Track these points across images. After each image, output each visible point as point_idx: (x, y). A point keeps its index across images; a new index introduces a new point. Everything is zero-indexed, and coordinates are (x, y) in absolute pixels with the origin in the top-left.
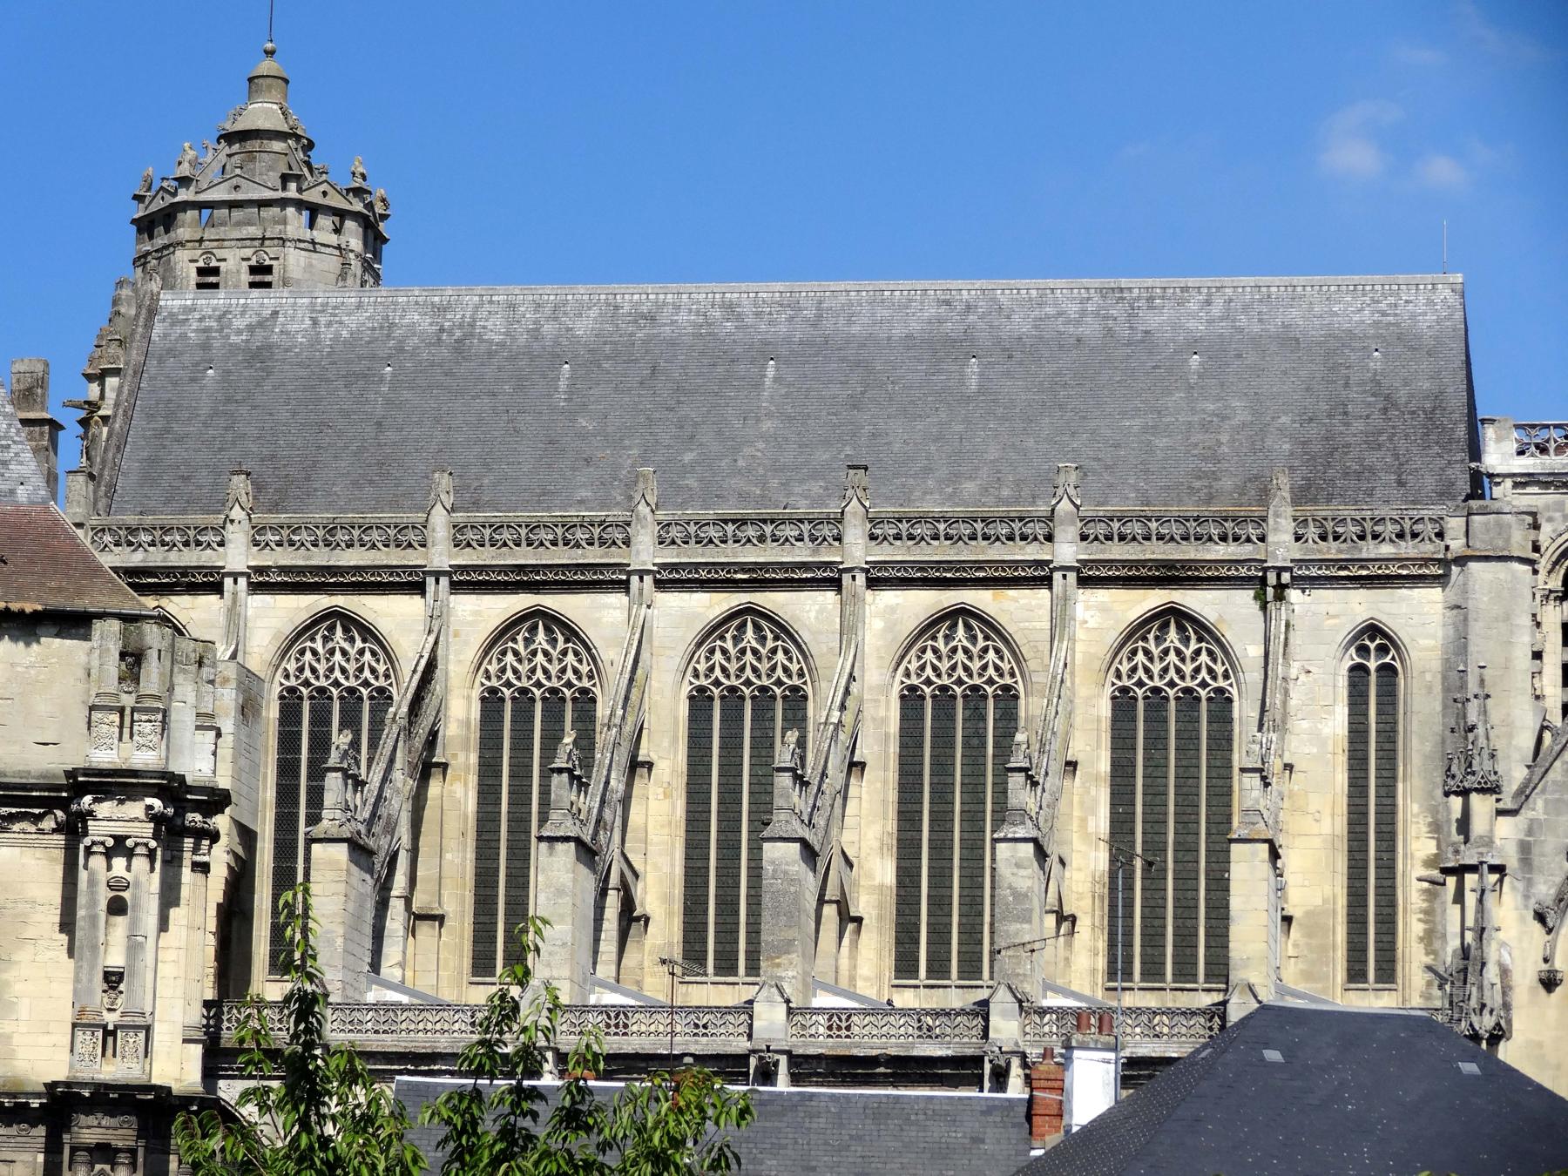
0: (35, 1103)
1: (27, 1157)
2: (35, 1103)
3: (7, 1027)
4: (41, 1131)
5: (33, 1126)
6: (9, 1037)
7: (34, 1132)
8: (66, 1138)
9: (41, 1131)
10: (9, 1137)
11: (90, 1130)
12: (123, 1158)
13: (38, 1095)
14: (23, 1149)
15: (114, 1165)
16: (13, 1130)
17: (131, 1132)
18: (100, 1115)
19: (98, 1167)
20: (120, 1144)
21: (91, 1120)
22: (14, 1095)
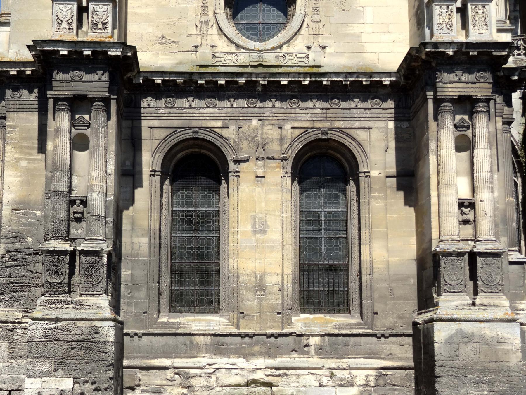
0: (386, 81)
1: (381, 124)
2: (386, 81)
3: (355, 29)
4: (390, 104)
5: (384, 100)
6: (359, 36)
7: (385, 105)
8: (430, 94)
9: (390, 104)
10: (365, 109)
11: (453, 84)
12: (481, 106)
13: (389, 74)
14: (377, 118)
15: (472, 114)
16: (368, 104)
17: (487, 85)
18: (459, 73)
19: (458, 117)
20: (479, 95)
21: (452, 77)
22: (370, 75)
